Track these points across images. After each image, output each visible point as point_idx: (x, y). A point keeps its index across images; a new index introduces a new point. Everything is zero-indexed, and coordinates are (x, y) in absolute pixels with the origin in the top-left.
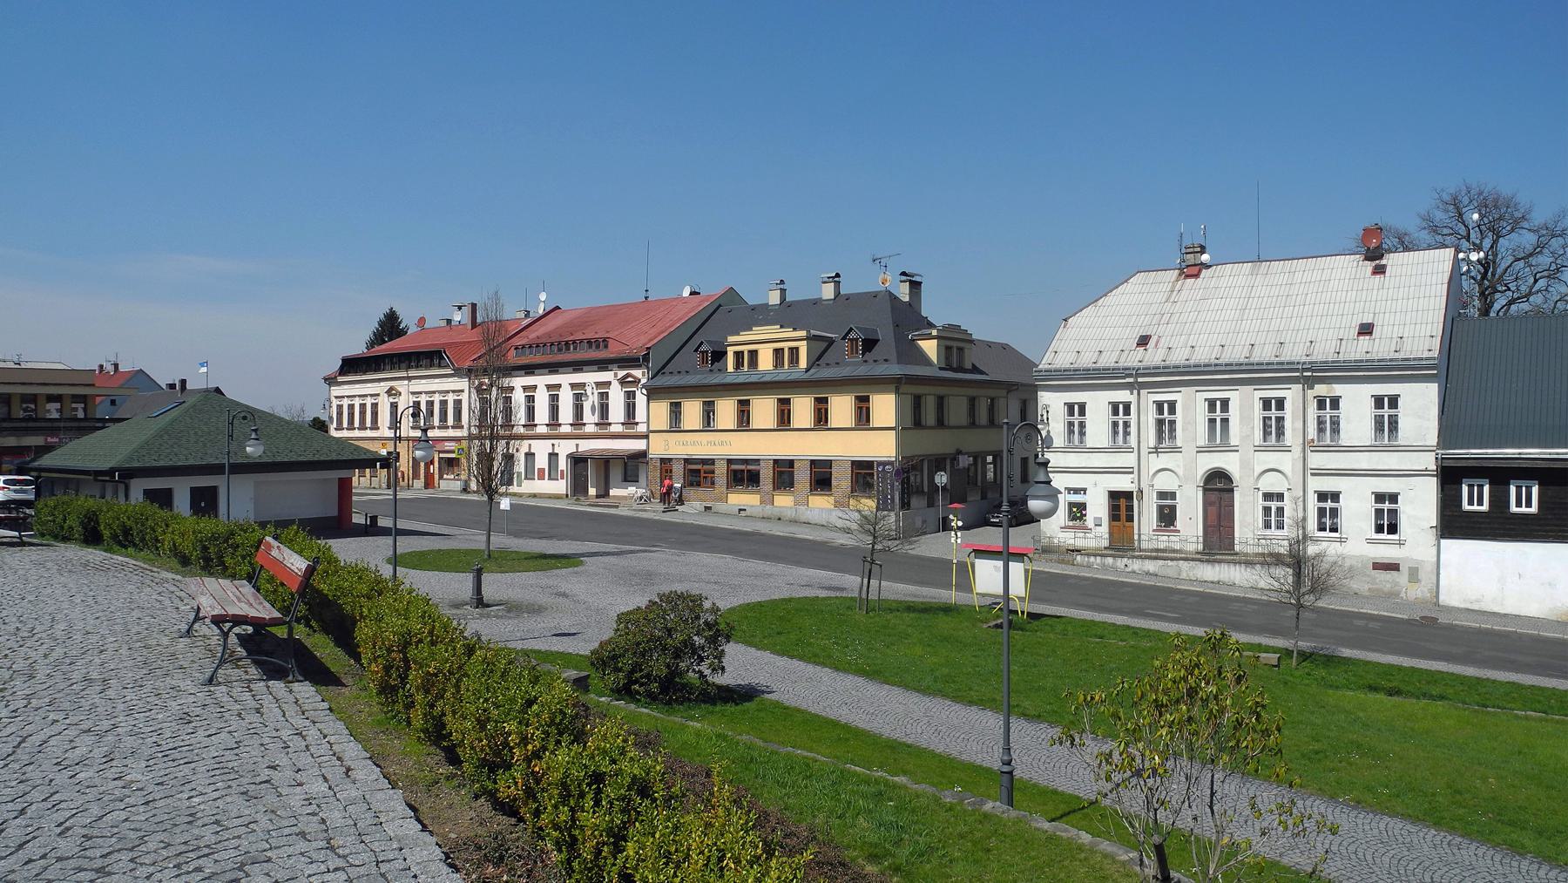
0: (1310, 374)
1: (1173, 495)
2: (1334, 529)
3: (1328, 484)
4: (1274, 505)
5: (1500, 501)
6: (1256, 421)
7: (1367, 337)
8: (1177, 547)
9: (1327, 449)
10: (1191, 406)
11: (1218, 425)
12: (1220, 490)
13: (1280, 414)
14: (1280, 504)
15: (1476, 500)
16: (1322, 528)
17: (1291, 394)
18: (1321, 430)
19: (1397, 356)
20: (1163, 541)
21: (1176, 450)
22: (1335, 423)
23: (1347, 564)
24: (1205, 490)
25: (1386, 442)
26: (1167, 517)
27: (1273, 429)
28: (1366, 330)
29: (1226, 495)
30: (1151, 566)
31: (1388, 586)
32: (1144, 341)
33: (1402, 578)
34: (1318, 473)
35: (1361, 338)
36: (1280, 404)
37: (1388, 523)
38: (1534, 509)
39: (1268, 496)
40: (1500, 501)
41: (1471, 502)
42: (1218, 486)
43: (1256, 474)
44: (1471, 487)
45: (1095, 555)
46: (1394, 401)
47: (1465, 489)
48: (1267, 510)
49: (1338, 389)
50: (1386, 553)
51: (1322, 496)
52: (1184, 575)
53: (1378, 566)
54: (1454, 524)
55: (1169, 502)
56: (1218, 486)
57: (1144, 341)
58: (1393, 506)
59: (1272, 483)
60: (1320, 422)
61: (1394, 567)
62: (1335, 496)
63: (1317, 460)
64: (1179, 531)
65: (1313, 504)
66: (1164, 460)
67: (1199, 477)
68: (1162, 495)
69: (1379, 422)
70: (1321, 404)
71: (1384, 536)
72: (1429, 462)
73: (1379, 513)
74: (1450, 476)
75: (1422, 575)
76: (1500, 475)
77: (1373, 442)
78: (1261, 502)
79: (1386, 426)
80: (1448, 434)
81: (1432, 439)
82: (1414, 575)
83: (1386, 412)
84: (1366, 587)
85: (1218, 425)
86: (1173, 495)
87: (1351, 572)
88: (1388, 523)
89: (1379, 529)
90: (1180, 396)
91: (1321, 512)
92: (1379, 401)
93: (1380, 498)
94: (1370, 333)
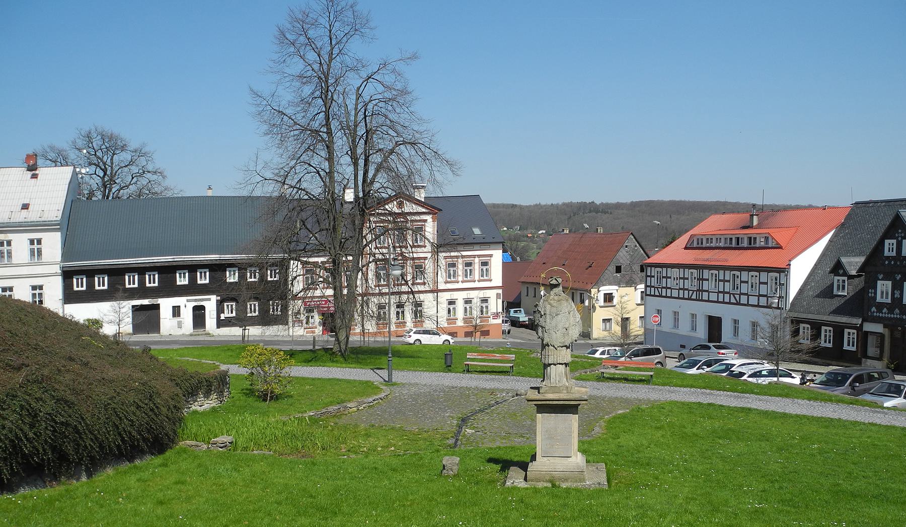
5: (91, 285)
7: (26, 210)
15: (79, 285)
19: (40, 220)
25: (36, 261)
28: (25, 207)
35: (23, 211)
38: (106, 287)
40: (91, 285)
41: (78, 286)
44: (77, 279)
46: (39, 242)
47: (75, 280)
49: (10, 236)
58: (41, 291)
69: (32, 251)
72: (57, 269)
74: (68, 275)
76: (90, 273)
77: (30, 262)
79: (36, 253)
80: (66, 256)
81: (59, 258)
83: (36, 246)
92: (32, 242)
93: (34, 288)
94: (27, 209)
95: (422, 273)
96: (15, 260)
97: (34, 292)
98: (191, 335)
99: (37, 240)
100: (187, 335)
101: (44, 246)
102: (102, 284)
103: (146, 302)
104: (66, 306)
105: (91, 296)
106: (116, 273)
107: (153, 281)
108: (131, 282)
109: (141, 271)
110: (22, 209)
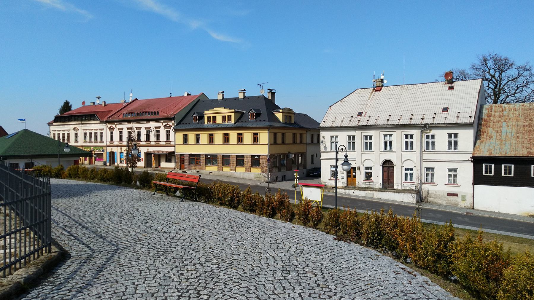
0: (424, 127)
1: (371, 169)
4: (409, 172)
5: (498, 171)
6: (403, 142)
7: (446, 113)
8: (372, 187)
9: (430, 153)
10: (378, 137)
11: (388, 145)
12: (389, 167)
13: (407, 140)
14: (411, 172)
17: (416, 133)
20: (367, 184)
21: (373, 152)
24: (383, 167)
26: (369, 176)
27: (408, 145)
28: (445, 110)
29: (391, 169)
30: (363, 193)
32: (360, 114)
33: (458, 199)
34: (426, 161)
35: (443, 113)
36: (412, 137)
39: (406, 169)
40: (498, 171)
42: (388, 166)
43: (403, 161)
45: (342, 189)
46: (456, 136)
48: (406, 174)
49: (433, 132)
50: (453, 190)
51: (428, 169)
52: (375, 197)
53: (449, 195)
55: (369, 171)
56: (388, 166)
57: (360, 114)
59: (408, 165)
60: (427, 143)
61: (456, 195)
63: (425, 156)
64: (373, 181)
65: (424, 172)
66: (365, 156)
67: (381, 162)
68: (367, 168)
69: (450, 143)
70: (428, 137)
72: (468, 157)
74: (477, 161)
78: (404, 172)
79: (453, 145)
82: (464, 198)
83: (453, 140)
85: (388, 145)
86: (371, 169)
87: (439, 197)
90: (374, 133)
91: (427, 175)
92: (450, 136)
93: (450, 170)
94: (447, 111)
97: (450, 173)
99: (454, 135)
101: (459, 139)
104: (476, 186)
110: (443, 111)
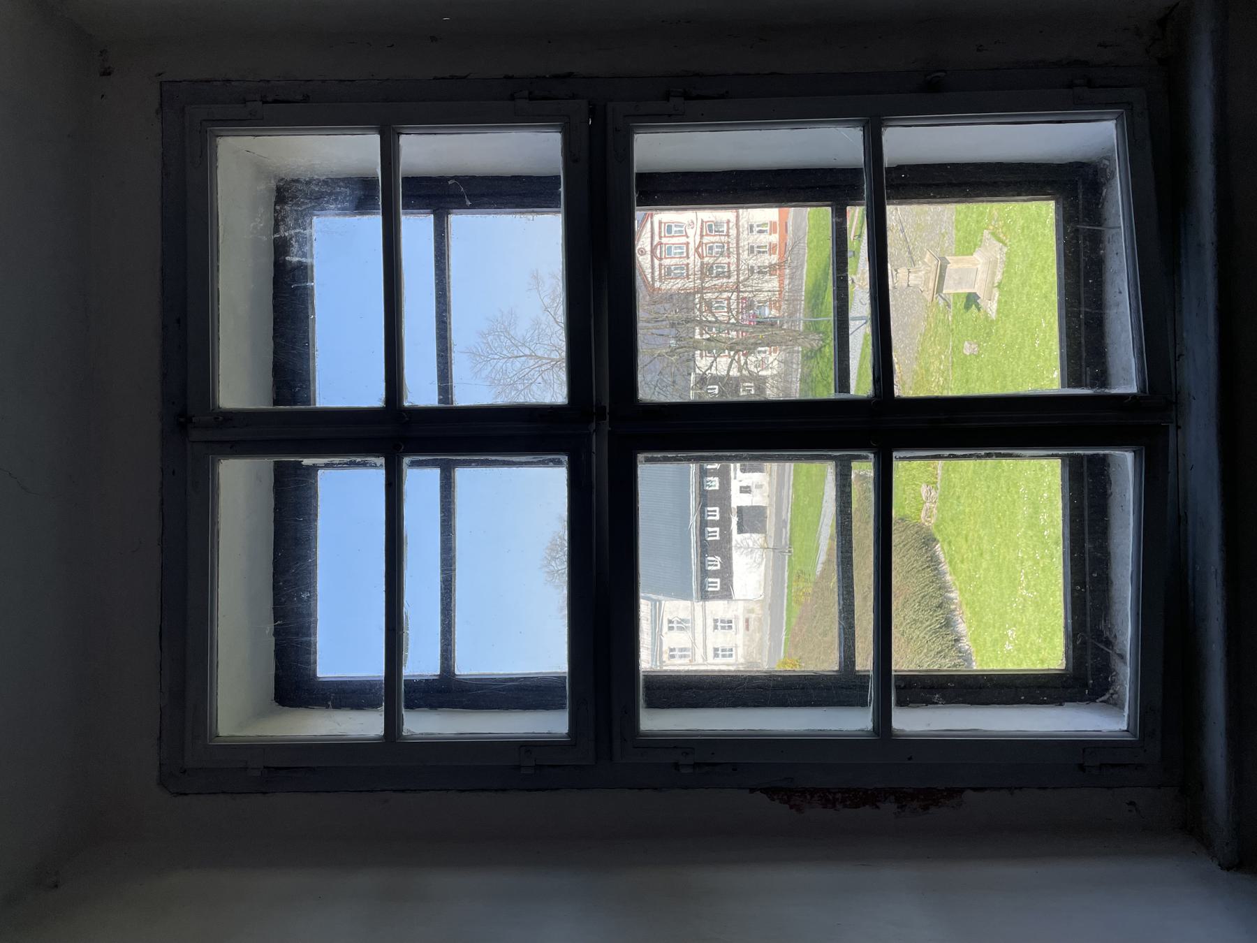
2: (731, 650)
3: (710, 653)
5: (715, 574)
9: (694, 654)
15: (715, 584)
16: (731, 656)
18: (685, 656)
22: (681, 650)
23: (747, 643)
25: (690, 625)
31: (756, 623)
37: (728, 624)
40: (715, 574)
41: (716, 587)
49: (665, 648)
50: (741, 624)
51: (716, 655)
53: (747, 628)
54: (726, 592)
60: (681, 657)
61: (747, 621)
62: (716, 650)
69: (681, 629)
70: (672, 657)
71: (733, 625)
72: (698, 605)
73: (723, 628)
74: (705, 595)
75: (751, 607)
76: (704, 573)
79: (681, 625)
80: (684, 594)
81: (688, 603)
82: (751, 611)
83: (675, 625)
84: (758, 635)
88: (728, 624)
89: (730, 627)
91: (724, 656)
92: (671, 628)
93: (716, 627)
95: (716, 224)
96: (689, 645)
97: (719, 628)
98: (770, 475)
100: (771, 479)
102: (715, 563)
103: (735, 520)
105: (726, 573)
106: (705, 548)
107: (714, 513)
108: (714, 534)
109: (703, 524)
